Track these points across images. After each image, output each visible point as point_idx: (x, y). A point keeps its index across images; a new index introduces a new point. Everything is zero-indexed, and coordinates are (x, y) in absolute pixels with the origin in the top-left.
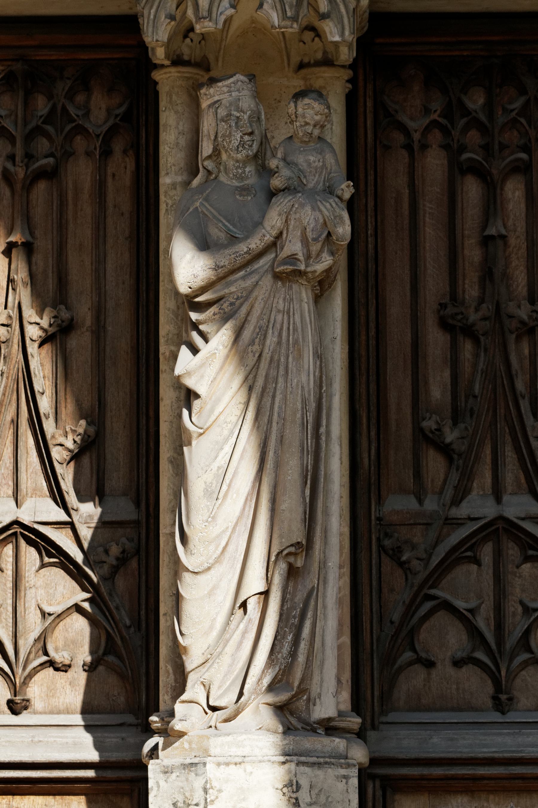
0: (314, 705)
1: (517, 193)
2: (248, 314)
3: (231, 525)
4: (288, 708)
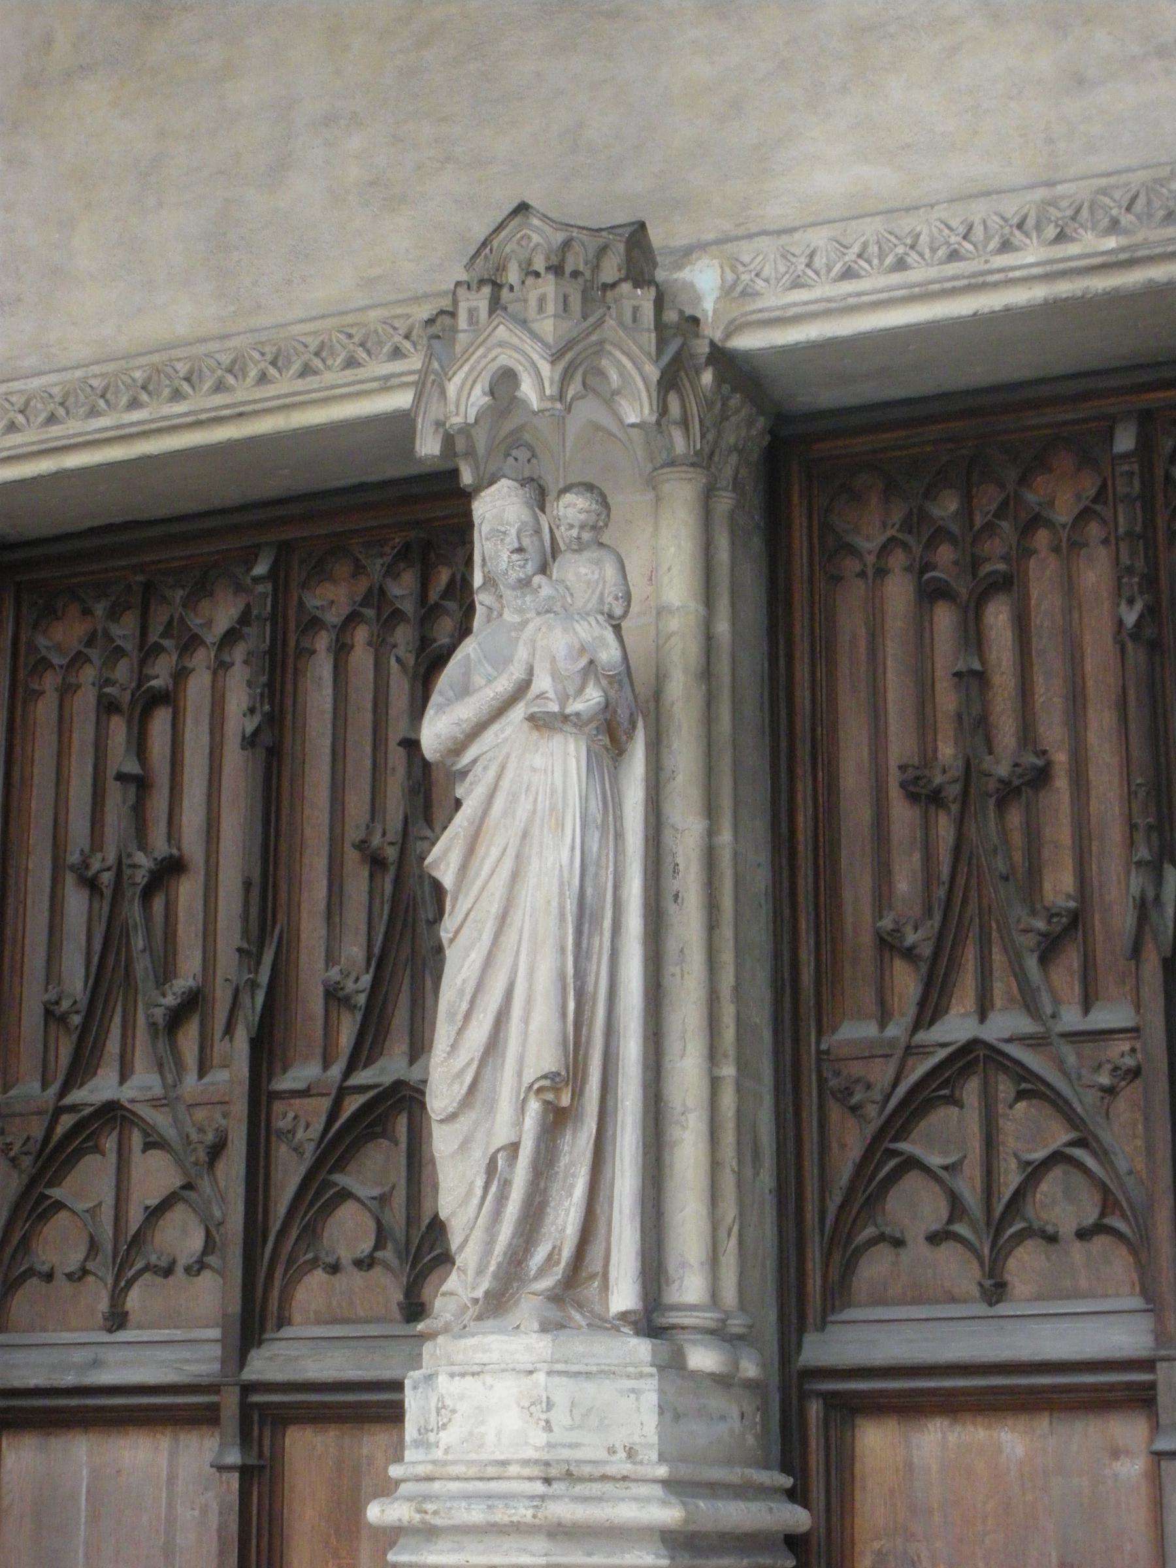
1: (1001, 616)
2: (499, 777)
3: (477, 1055)
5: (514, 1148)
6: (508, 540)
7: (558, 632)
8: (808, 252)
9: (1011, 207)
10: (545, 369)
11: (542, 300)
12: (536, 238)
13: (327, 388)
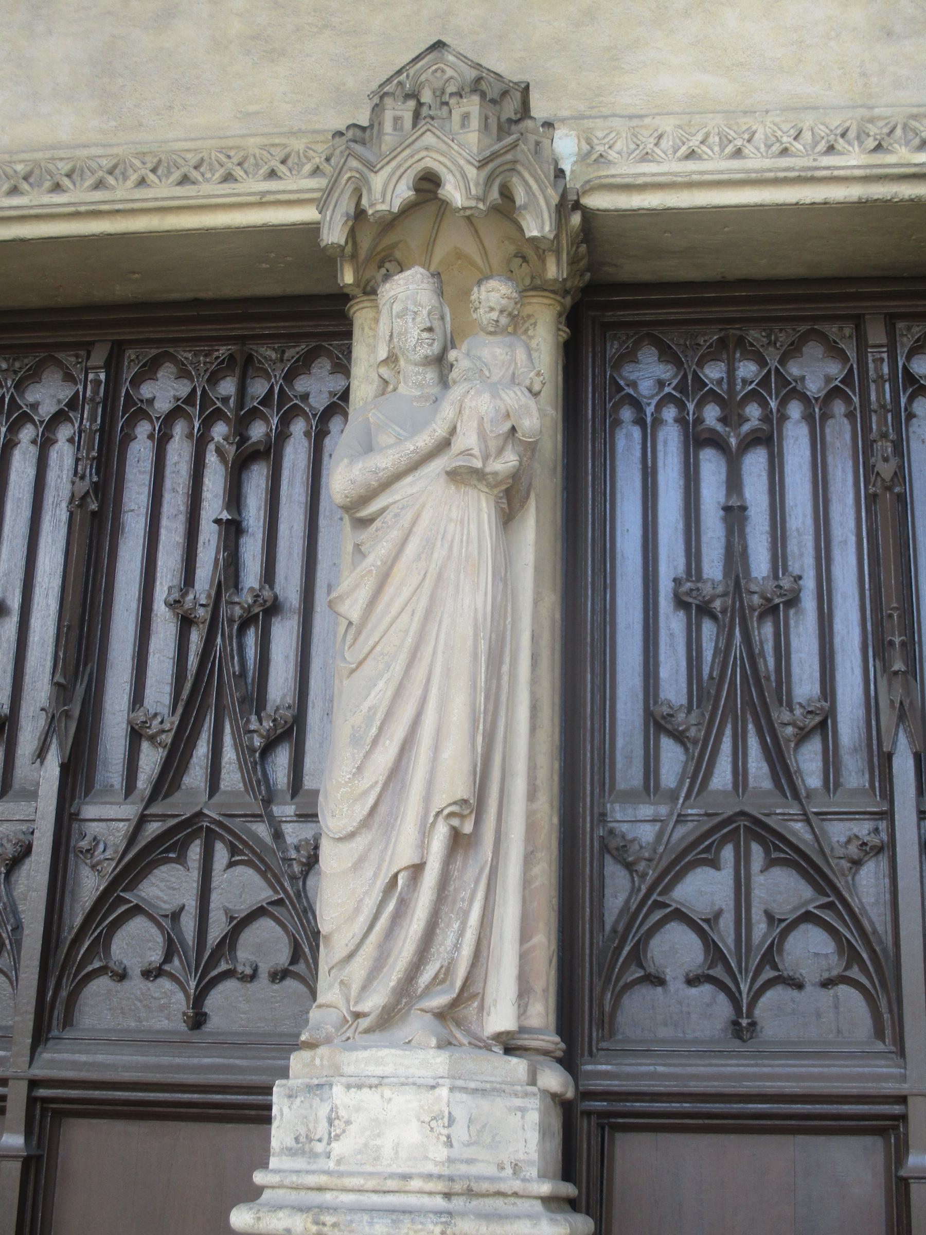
0: (488, 1015)
3: (382, 780)
4: (453, 1019)
5: (417, 869)
6: (419, 319)
7: (486, 397)
8: (656, 135)
9: (836, 121)
10: (472, 172)
11: (466, 117)
12: (450, 72)
13: (204, 197)
